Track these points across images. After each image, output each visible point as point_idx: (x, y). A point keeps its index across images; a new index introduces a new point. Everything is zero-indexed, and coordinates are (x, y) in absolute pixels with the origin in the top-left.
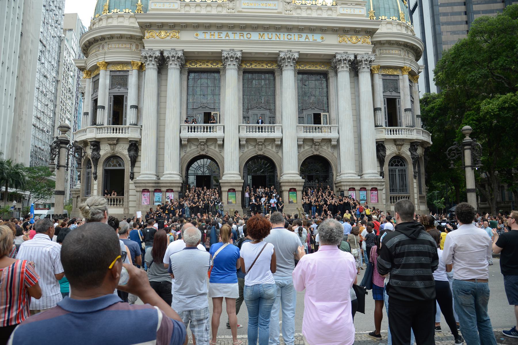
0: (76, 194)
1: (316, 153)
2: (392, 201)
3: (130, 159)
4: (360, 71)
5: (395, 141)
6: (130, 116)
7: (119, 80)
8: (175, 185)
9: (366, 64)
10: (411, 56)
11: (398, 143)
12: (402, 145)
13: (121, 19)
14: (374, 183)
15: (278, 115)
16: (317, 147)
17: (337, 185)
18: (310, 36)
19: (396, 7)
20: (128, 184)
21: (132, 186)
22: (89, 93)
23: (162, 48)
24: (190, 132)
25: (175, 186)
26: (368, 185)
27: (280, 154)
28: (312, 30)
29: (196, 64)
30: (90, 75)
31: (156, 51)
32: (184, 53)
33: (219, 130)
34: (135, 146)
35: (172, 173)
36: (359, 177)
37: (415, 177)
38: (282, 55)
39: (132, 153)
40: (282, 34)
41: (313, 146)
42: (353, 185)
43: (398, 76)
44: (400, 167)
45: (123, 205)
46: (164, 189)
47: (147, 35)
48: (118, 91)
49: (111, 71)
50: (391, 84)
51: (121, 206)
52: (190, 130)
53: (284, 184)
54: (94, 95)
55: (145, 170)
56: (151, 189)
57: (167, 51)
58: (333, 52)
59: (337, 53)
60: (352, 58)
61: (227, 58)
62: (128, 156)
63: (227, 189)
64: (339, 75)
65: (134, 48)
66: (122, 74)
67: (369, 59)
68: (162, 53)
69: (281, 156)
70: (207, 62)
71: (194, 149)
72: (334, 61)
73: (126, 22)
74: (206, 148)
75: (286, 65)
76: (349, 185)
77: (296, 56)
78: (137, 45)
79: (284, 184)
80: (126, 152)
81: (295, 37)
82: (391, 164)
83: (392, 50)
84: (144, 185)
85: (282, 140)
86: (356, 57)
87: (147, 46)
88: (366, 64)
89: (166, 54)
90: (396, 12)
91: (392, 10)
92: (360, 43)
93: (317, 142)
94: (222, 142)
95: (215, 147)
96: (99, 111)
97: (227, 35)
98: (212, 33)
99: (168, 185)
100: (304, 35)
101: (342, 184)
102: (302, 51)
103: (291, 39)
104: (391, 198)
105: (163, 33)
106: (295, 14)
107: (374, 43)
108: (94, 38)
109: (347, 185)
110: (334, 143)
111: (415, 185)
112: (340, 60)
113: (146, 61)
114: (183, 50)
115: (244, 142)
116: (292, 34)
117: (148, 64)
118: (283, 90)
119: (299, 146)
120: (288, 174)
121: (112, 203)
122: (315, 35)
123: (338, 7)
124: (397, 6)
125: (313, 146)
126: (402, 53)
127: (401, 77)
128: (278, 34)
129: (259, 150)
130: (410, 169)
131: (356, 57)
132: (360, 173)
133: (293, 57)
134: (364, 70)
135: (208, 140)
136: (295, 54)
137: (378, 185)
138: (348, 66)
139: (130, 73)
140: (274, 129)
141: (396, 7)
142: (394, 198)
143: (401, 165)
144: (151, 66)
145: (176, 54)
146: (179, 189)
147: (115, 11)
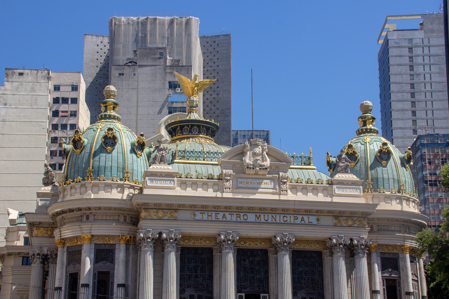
18: (306, 218)
29: (190, 241)
40: (278, 216)
48: (103, 266)
49: (95, 244)
66: (107, 247)
70: (201, 239)
78: (125, 217)
81: (290, 219)
83: (391, 226)
86: (351, 240)
91: (391, 181)
92: (355, 225)
97: (224, 216)
98: (210, 214)
100: (300, 217)
103: (287, 221)
116: (288, 216)
123: (335, 186)
127: (401, 256)
128: (274, 215)
131: (351, 240)
138: (344, 250)
139: (117, 247)
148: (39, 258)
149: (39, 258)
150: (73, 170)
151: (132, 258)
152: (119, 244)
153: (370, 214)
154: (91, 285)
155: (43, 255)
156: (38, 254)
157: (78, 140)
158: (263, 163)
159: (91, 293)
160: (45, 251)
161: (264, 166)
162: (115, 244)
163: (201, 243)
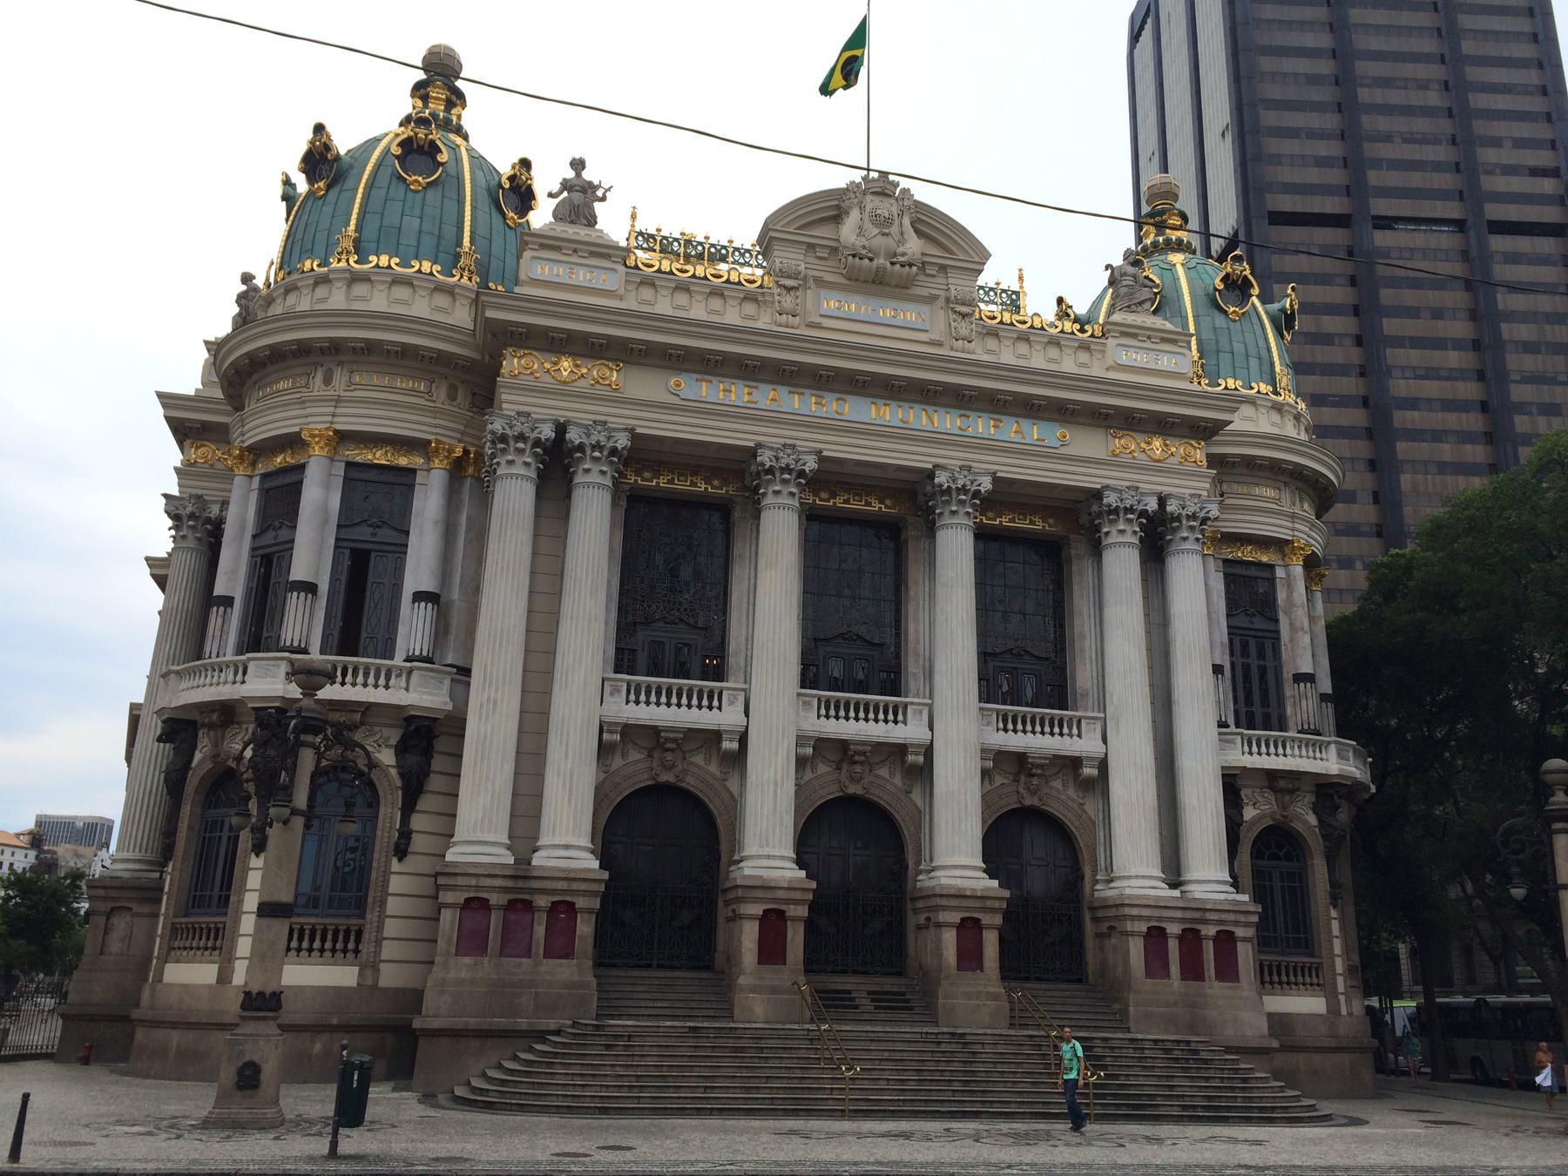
0: (105, 899)
1: (1028, 802)
2: (1267, 979)
3: (399, 783)
4: (1173, 547)
5: (1272, 778)
6: (413, 630)
7: (376, 497)
8: (583, 886)
9: (1192, 528)
10: (1306, 506)
11: (1282, 784)
12: (1292, 792)
13: (401, 292)
14: (1224, 916)
15: (912, 667)
16: (1035, 781)
17: (1100, 914)
18: (1025, 424)
19: (1264, 353)
20: (387, 874)
21: (396, 884)
22: (243, 527)
23: (562, 416)
24: (632, 704)
25: (586, 893)
26: (1205, 922)
27: (917, 796)
28: (1029, 408)
29: (657, 475)
30: (253, 464)
31: (544, 421)
32: (635, 437)
33: (731, 703)
34: (429, 742)
35: (568, 843)
36: (1176, 893)
37: (1334, 900)
38: (942, 478)
39: (412, 760)
41: (1023, 778)
42: (1160, 919)
43: (1271, 567)
44: (1284, 863)
45: (356, 951)
46: (542, 902)
47: (513, 364)
50: (1249, 596)
51: (350, 955)
52: (632, 697)
53: (944, 902)
54: (268, 538)
55: (478, 829)
56: (495, 899)
57: (578, 425)
58: (1096, 484)
59: (1107, 487)
60: (1152, 505)
61: (770, 471)
62: (393, 772)
63: (757, 909)
64: (1109, 557)
65: (441, 394)
67: (1202, 514)
68: (561, 429)
69: (919, 802)
70: (694, 474)
71: (637, 762)
72: (1095, 508)
73: (420, 307)
74: (679, 763)
75: (954, 513)
76: (1149, 918)
77: (986, 484)
79: (944, 902)
80: (387, 757)
81: (982, 426)
82: (1256, 854)
83: (1257, 485)
84: (473, 882)
85: (929, 751)
86: (1162, 501)
87: (509, 402)
88: (1192, 528)
89: (573, 435)
90: (1266, 368)
91: (1254, 362)
93: (1041, 766)
94: (735, 745)
95: (708, 761)
96: (295, 604)
99: (560, 885)
101: (1127, 911)
102: (1006, 473)
104: (1261, 966)
105: (566, 364)
106: (980, 352)
107: (1215, 461)
108: (298, 341)
109: (1140, 918)
110: (1089, 771)
111: (1335, 925)
112: (1116, 511)
113: (503, 451)
114: (631, 431)
115: (809, 751)
116: (972, 414)
117: (510, 462)
118: (939, 590)
119: (985, 773)
120: (956, 867)
121: (317, 944)
122: (1043, 424)
123: (1111, 342)
124: (1269, 350)
125: (1023, 778)
126: (1286, 497)
127: (1280, 573)
129: (852, 779)
130: (1319, 871)
131: (1162, 501)
132: (1174, 873)
133: (974, 488)
134: (1187, 545)
135: (692, 733)
136: (981, 479)
137: (1236, 923)
139: (420, 478)
140: (905, 714)
141: (1264, 353)
142: (1270, 967)
143: (1288, 858)
144: (519, 469)
145: (609, 438)
146: (597, 903)
147: (384, 261)
148: (193, 527)
149: (193, 527)
150: (297, 247)
151: (469, 518)
152: (428, 471)
153: (1218, 426)
154: (324, 588)
155: (208, 520)
156: (192, 516)
157: (321, 154)
158: (901, 250)
159: (320, 615)
160: (215, 511)
161: (903, 254)
162: (414, 471)
163: (693, 484)
